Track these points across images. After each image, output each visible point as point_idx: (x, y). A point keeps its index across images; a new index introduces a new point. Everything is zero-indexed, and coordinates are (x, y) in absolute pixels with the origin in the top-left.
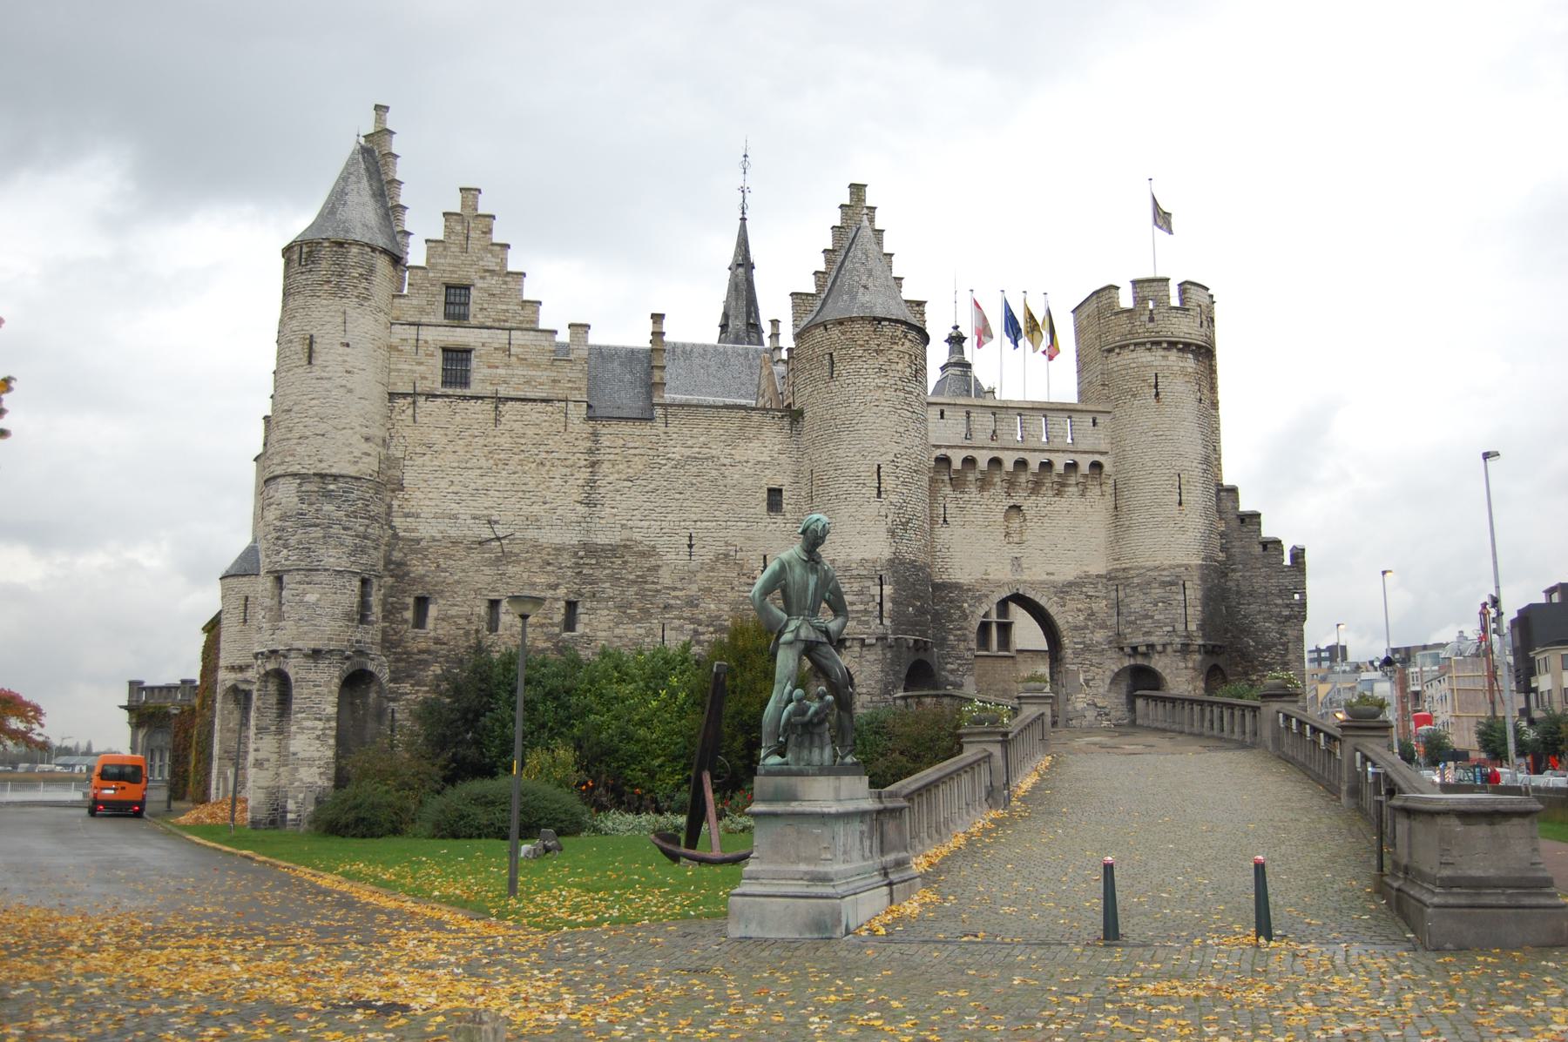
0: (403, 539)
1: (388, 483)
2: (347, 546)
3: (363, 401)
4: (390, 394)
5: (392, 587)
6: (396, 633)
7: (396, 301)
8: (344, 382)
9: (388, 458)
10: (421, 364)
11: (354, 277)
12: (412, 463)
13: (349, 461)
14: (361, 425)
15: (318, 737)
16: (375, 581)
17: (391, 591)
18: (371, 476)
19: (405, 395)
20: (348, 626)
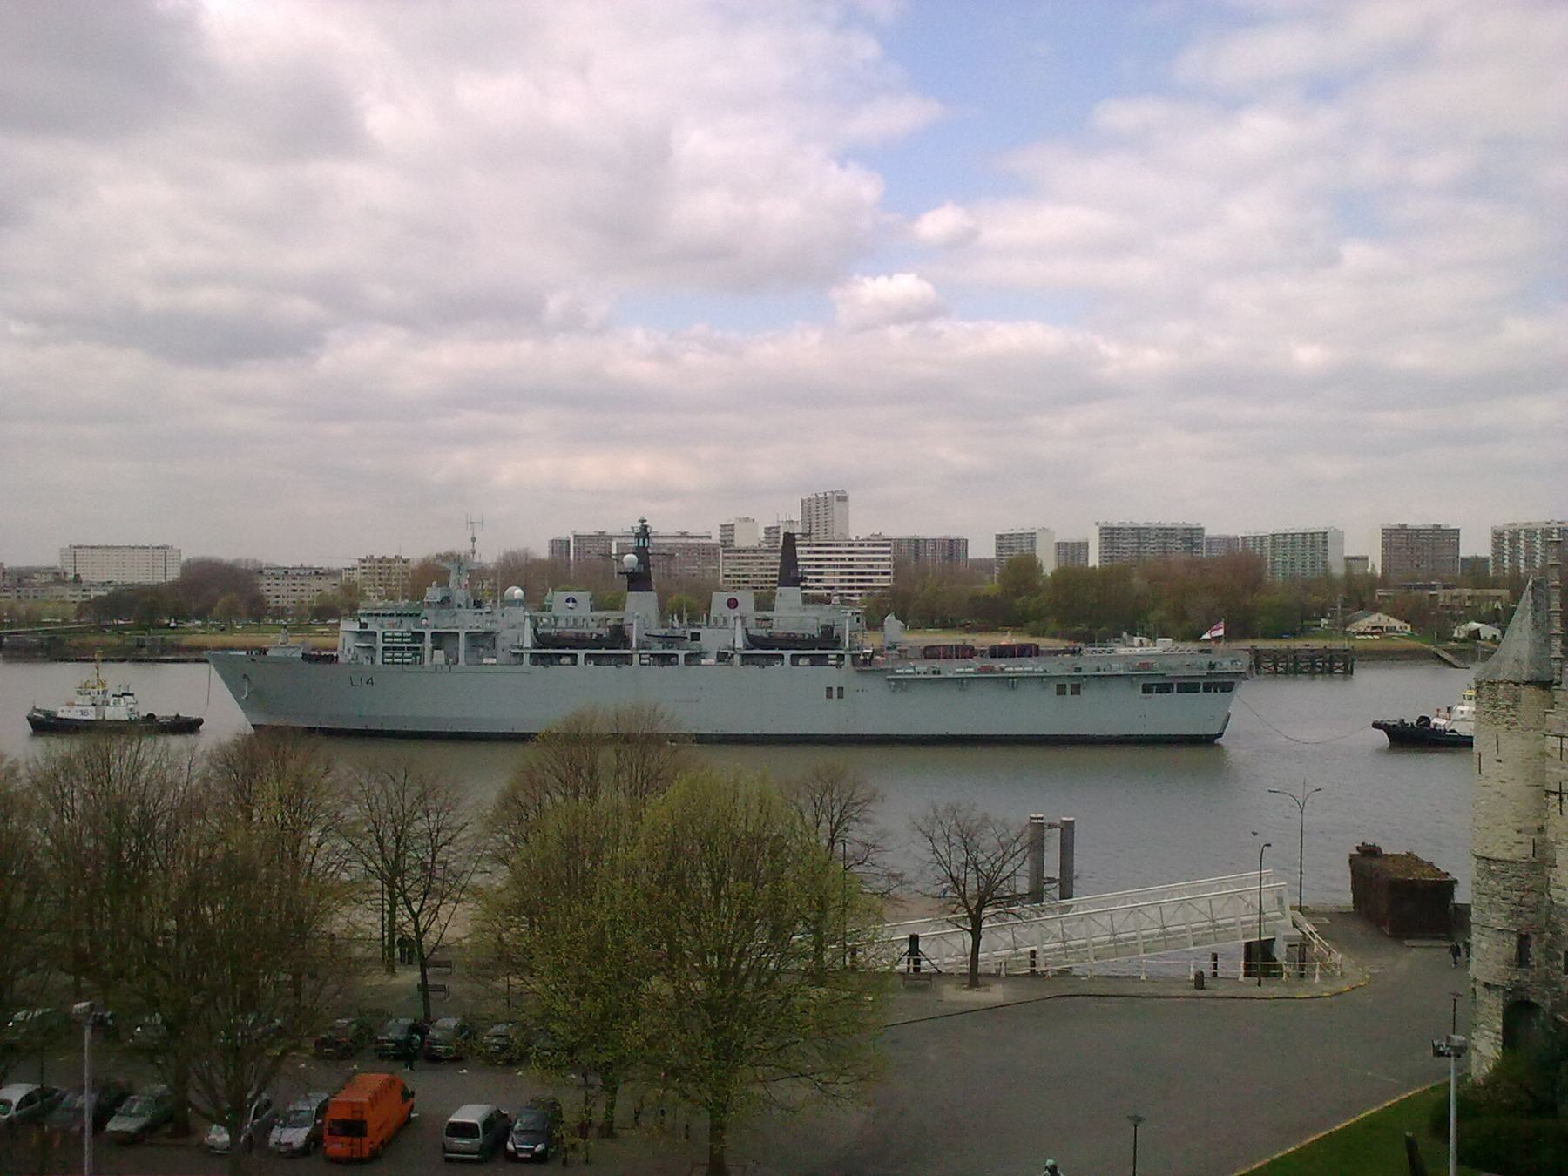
0: (1560, 907)
1: (1540, 861)
2: (1505, 912)
3: (1513, 803)
4: (1547, 791)
5: (1550, 941)
6: (1554, 976)
7: (1547, 716)
8: (1499, 790)
9: (1545, 841)
10: (1563, 768)
11: (1503, 708)
12: (1560, 846)
13: (1504, 849)
14: (1512, 822)
15: (1492, 1044)
16: (1534, 938)
17: (1551, 944)
18: (1525, 858)
19: (1555, 793)
20: (1508, 970)
